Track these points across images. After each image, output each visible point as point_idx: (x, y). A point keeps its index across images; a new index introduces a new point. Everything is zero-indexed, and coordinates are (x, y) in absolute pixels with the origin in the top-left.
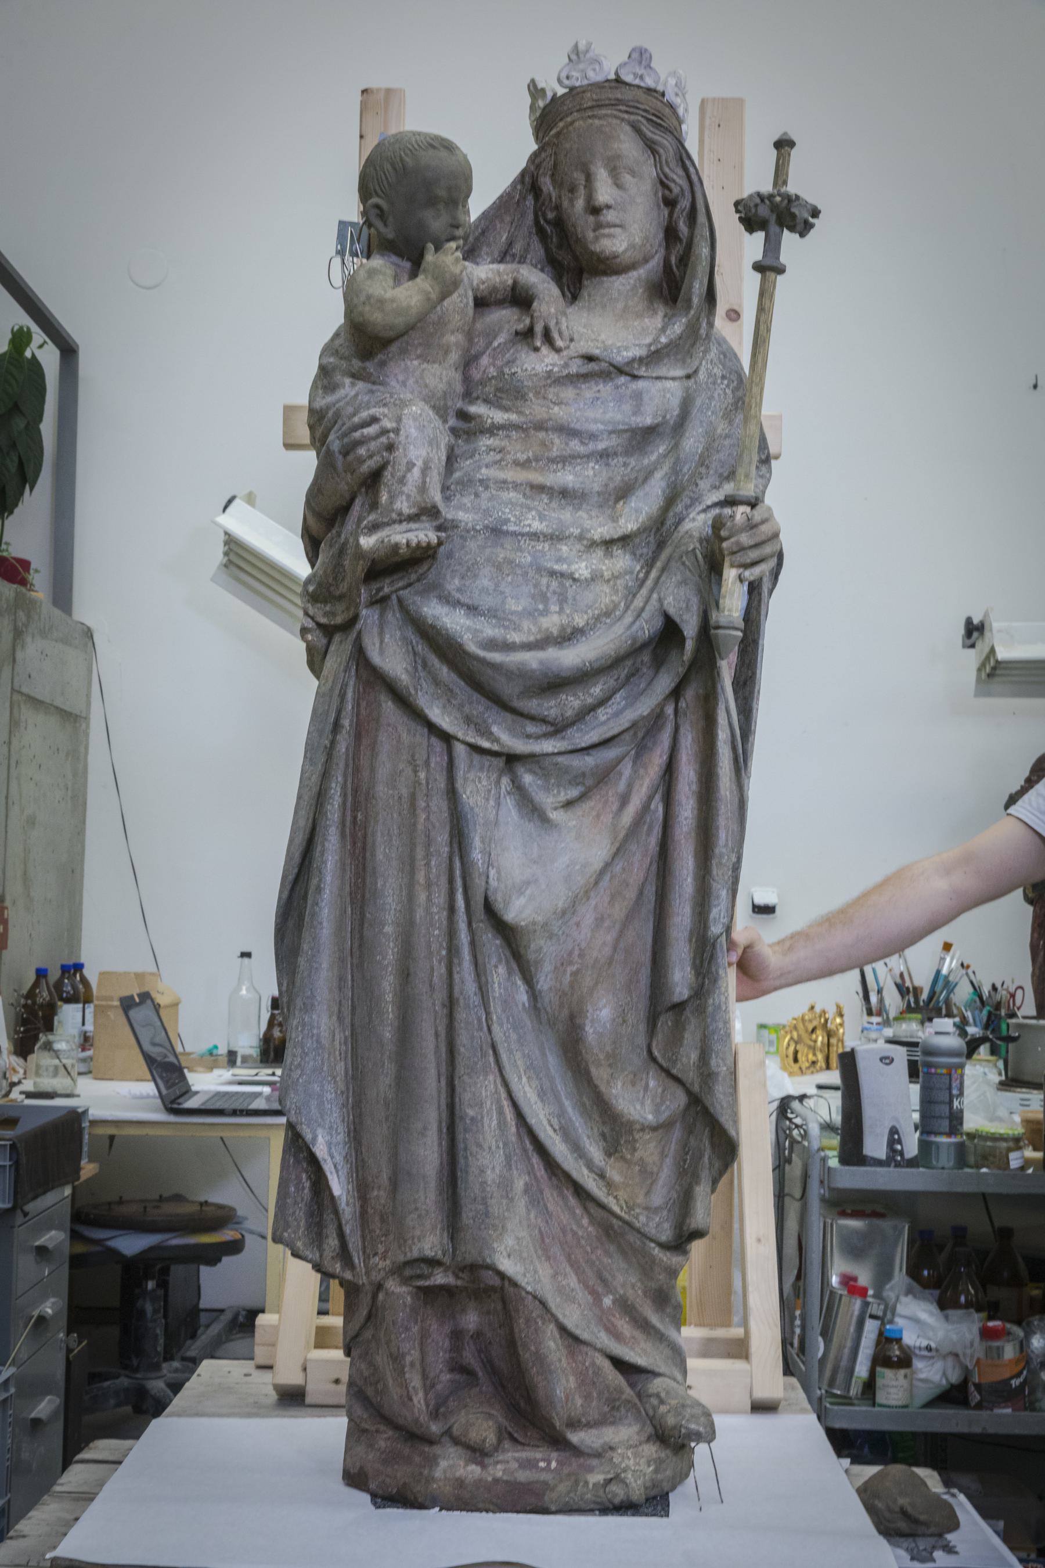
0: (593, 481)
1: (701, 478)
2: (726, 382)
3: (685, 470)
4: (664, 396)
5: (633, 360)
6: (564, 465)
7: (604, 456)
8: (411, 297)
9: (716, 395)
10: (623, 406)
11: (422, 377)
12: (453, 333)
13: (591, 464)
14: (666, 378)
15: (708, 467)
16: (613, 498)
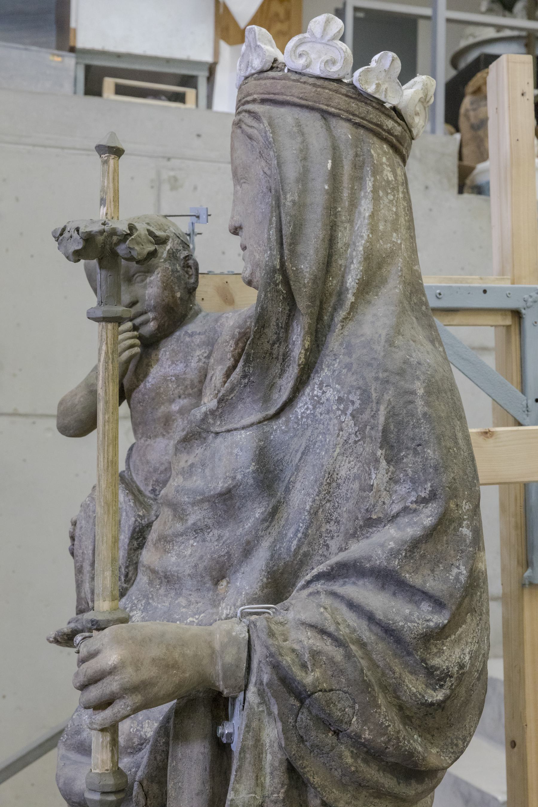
0: (187, 563)
1: (332, 538)
2: (342, 407)
3: (290, 535)
4: (231, 453)
5: (206, 414)
6: (173, 544)
7: (198, 530)
8: (76, 395)
9: (331, 427)
10: (206, 471)
11: (144, 455)
12: (172, 401)
13: (191, 542)
14: (236, 429)
15: (338, 522)
16: (207, 578)
